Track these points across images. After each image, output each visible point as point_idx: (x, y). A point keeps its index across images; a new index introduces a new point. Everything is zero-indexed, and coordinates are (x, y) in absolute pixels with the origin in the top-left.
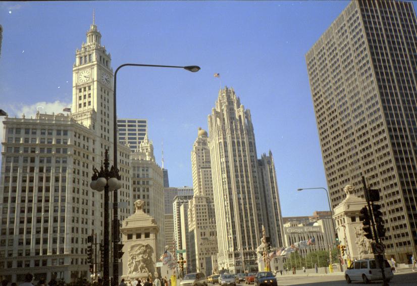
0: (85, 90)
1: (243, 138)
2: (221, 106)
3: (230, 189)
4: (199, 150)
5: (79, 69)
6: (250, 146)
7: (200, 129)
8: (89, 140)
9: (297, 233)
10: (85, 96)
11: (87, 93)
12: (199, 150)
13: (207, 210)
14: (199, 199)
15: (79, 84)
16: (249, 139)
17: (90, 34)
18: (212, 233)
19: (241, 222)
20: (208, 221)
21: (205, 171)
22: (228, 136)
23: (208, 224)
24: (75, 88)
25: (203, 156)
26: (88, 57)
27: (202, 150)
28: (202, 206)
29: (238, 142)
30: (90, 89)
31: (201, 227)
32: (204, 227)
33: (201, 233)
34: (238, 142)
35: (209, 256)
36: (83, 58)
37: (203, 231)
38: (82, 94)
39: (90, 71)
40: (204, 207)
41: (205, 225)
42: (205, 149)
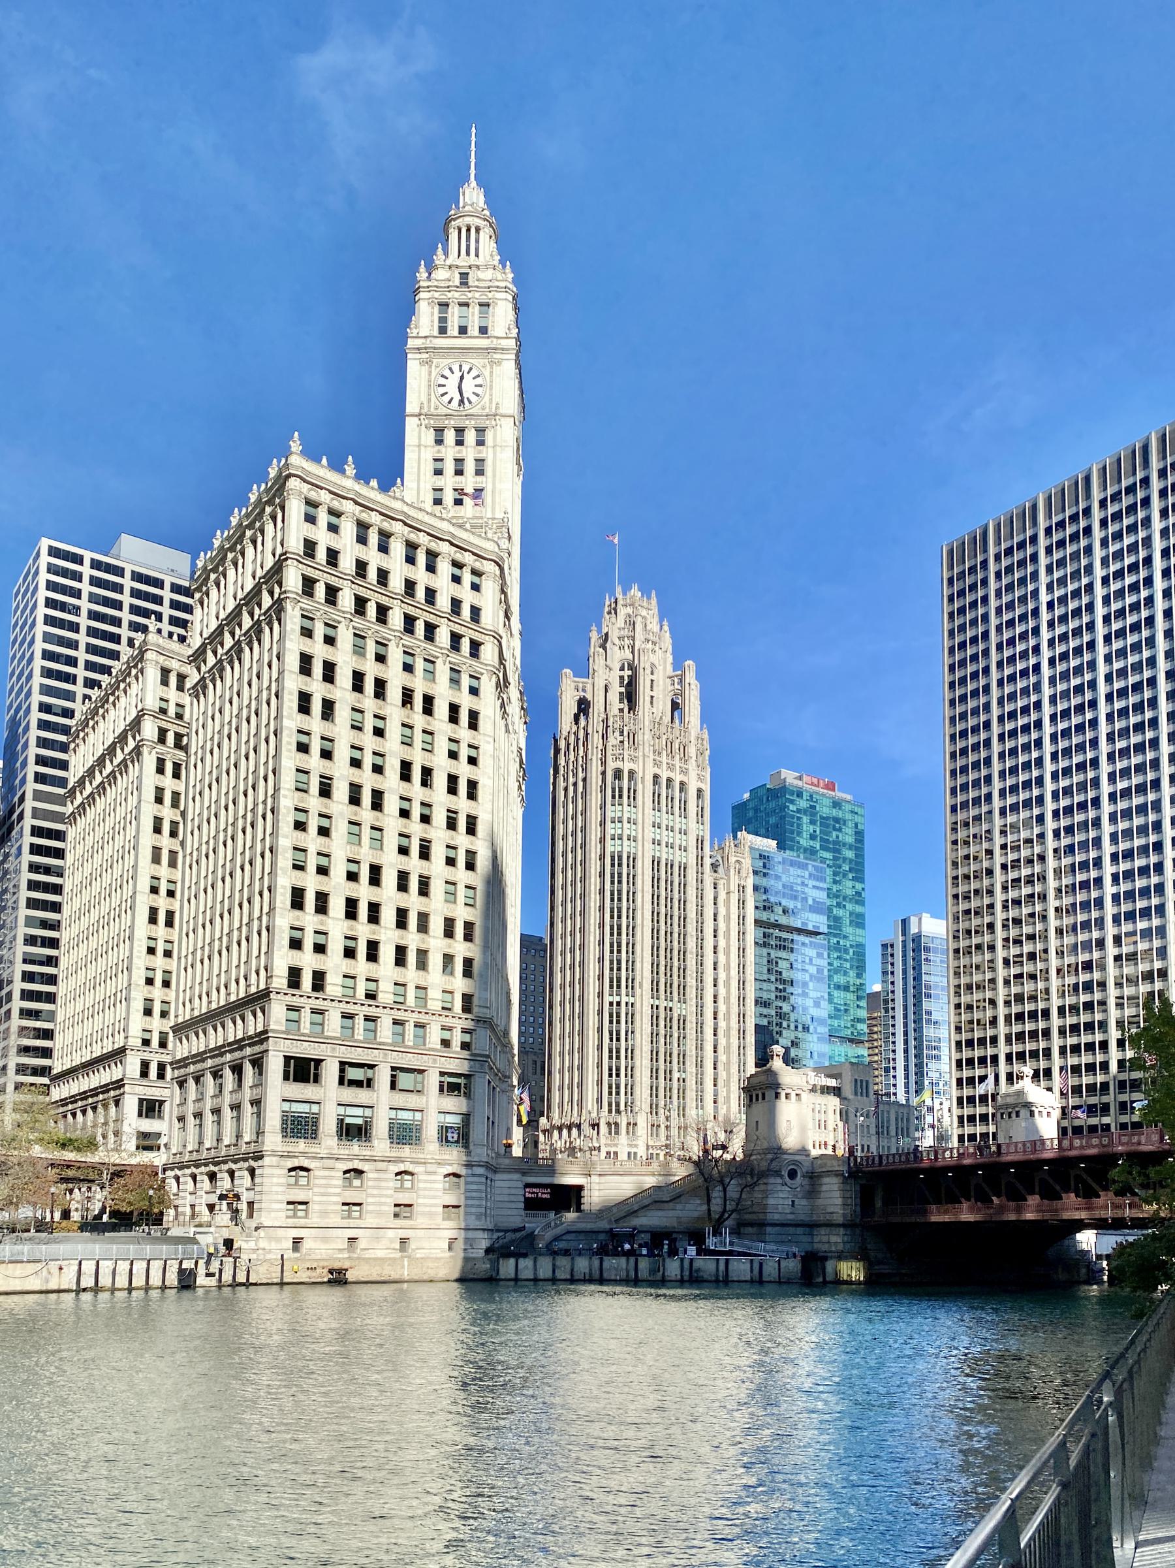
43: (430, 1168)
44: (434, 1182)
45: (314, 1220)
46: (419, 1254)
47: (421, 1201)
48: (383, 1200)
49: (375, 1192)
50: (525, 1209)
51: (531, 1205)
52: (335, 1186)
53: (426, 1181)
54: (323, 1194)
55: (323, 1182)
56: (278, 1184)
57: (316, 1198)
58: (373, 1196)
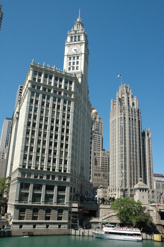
2: (122, 95)
5: (70, 44)
9: (161, 181)
10: (74, 63)
11: (75, 61)
15: (69, 54)
16: (139, 118)
18: (96, 174)
22: (127, 114)
24: (66, 57)
26: (77, 38)
29: (132, 119)
30: (78, 57)
34: (132, 119)
36: (74, 38)
39: (79, 47)
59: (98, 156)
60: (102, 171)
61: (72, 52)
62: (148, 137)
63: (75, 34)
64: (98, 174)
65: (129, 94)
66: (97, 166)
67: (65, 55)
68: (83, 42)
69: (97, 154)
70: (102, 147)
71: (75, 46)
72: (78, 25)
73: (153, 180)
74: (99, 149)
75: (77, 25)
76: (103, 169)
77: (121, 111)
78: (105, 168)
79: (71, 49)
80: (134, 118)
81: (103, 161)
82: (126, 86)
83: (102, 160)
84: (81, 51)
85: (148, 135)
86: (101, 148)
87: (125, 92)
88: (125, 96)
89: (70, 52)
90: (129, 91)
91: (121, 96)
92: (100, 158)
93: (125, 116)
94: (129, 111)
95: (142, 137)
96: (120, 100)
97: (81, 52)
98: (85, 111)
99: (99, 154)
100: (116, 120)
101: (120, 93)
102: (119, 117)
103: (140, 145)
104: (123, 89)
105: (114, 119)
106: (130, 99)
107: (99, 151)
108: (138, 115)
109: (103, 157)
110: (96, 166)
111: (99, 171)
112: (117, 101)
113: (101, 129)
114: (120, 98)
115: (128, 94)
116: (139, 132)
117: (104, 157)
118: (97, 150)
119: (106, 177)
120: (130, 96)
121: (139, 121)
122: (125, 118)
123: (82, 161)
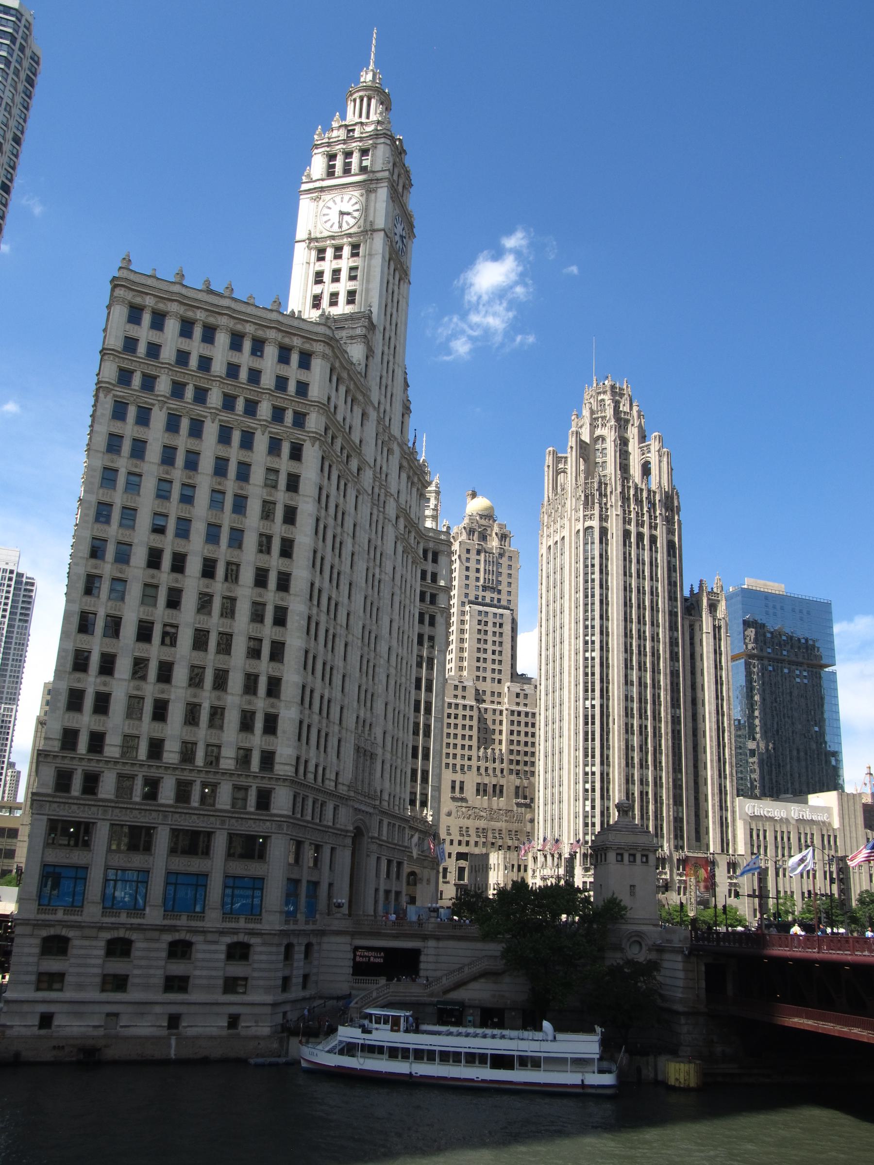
0: (338, 257)
1: (653, 527)
2: (593, 427)
3: (604, 664)
4: (468, 551)
5: (322, 189)
6: (669, 555)
7: (474, 495)
8: (355, 408)
9: (771, 819)
12: (468, 551)
13: (475, 723)
14: (456, 687)
15: (319, 236)
16: (670, 532)
17: (361, 93)
19: (627, 765)
20: (474, 752)
21: (480, 612)
22: (615, 513)
23: (474, 763)
24: (304, 245)
25: (478, 570)
27: (479, 553)
28: (465, 707)
29: (640, 536)
31: (454, 765)
32: (463, 766)
33: (454, 782)
34: (640, 536)
35: (484, 851)
37: (458, 777)
38: (328, 266)
40: (468, 713)
41: (466, 763)
42: (486, 552)
43: (210, 937)
44: (215, 952)
45: (68, 994)
46: (191, 1032)
47: (197, 973)
48: (152, 972)
49: (143, 963)
50: (353, 975)
51: (361, 969)
52: (96, 957)
53: (204, 951)
54: (79, 965)
55: (82, 952)
56: (29, 955)
57: (71, 970)
58: (140, 967)
59: (494, 706)
60: (511, 771)
61: (329, 224)
62: (714, 620)
63: (345, 142)
64: (495, 786)
65: (627, 421)
66: (489, 751)
67: (297, 239)
68: (379, 175)
69: (487, 697)
70: (513, 666)
71: (346, 198)
72: (365, 99)
73: (733, 812)
74: (497, 676)
75: (358, 101)
76: (518, 762)
77: (588, 503)
78: (526, 759)
79: (326, 211)
80: (646, 530)
81: (515, 728)
82: (613, 387)
83: (512, 722)
84: (371, 218)
85: (713, 607)
86: (506, 667)
87: (609, 412)
88: (608, 433)
89: (319, 226)
90: (626, 409)
91: (592, 432)
92: (501, 712)
93: (604, 524)
94: (625, 499)
95: (683, 619)
96: (585, 451)
97: (372, 224)
98: (388, 494)
99: (499, 694)
100: (567, 540)
101: (587, 421)
102: (580, 526)
103: (674, 657)
104: (603, 400)
105: (558, 538)
106: (633, 447)
107: (499, 681)
108: (669, 521)
109: (515, 708)
110: (482, 750)
111: (498, 772)
112: (572, 456)
113: (510, 584)
114: (588, 441)
115: (622, 423)
116: (672, 598)
117: (521, 708)
118: (489, 680)
119: (528, 801)
120: (632, 433)
121: (671, 545)
122: (604, 532)
123: (363, 724)
